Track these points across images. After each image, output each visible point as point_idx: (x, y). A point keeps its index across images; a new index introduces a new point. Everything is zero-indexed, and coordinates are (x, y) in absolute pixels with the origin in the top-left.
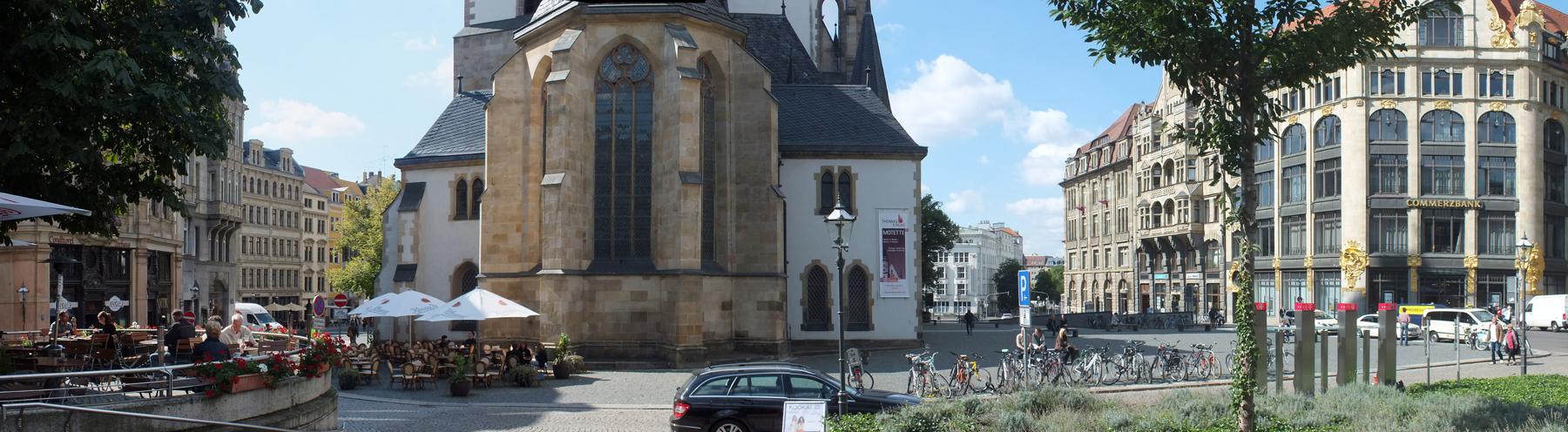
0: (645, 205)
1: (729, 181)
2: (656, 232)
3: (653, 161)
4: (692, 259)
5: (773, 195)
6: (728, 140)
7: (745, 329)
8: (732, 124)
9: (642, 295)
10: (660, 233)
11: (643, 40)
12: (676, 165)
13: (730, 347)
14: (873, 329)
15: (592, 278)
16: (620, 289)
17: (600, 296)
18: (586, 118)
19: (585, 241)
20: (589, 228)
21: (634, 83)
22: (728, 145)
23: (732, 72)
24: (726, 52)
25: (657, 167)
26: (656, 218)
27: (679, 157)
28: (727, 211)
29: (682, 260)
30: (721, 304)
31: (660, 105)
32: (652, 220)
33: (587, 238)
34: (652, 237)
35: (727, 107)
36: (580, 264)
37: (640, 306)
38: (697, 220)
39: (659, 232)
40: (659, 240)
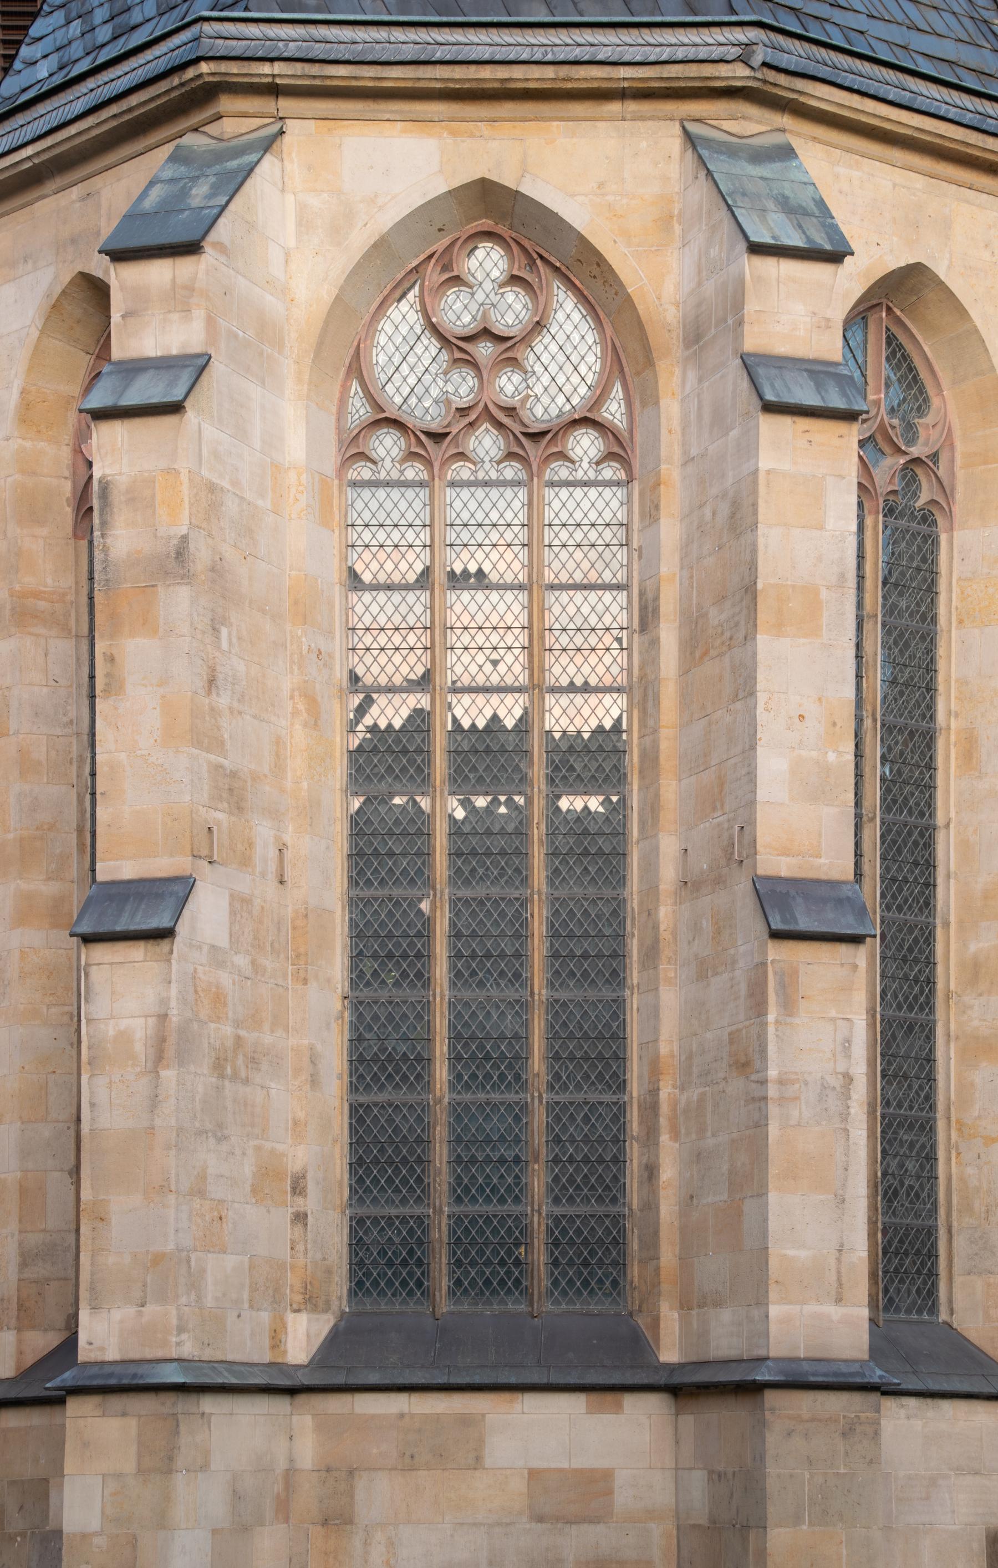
2: (651, 1171)
4: (834, 1312)
16: (478, 1463)
19: (300, 1218)
21: (536, 437)
26: (651, 1107)
27: (752, 803)
29: (775, 1311)
33: (311, 1203)
34: (634, 1196)
36: (277, 1337)
38: (845, 1116)
39: (668, 1173)
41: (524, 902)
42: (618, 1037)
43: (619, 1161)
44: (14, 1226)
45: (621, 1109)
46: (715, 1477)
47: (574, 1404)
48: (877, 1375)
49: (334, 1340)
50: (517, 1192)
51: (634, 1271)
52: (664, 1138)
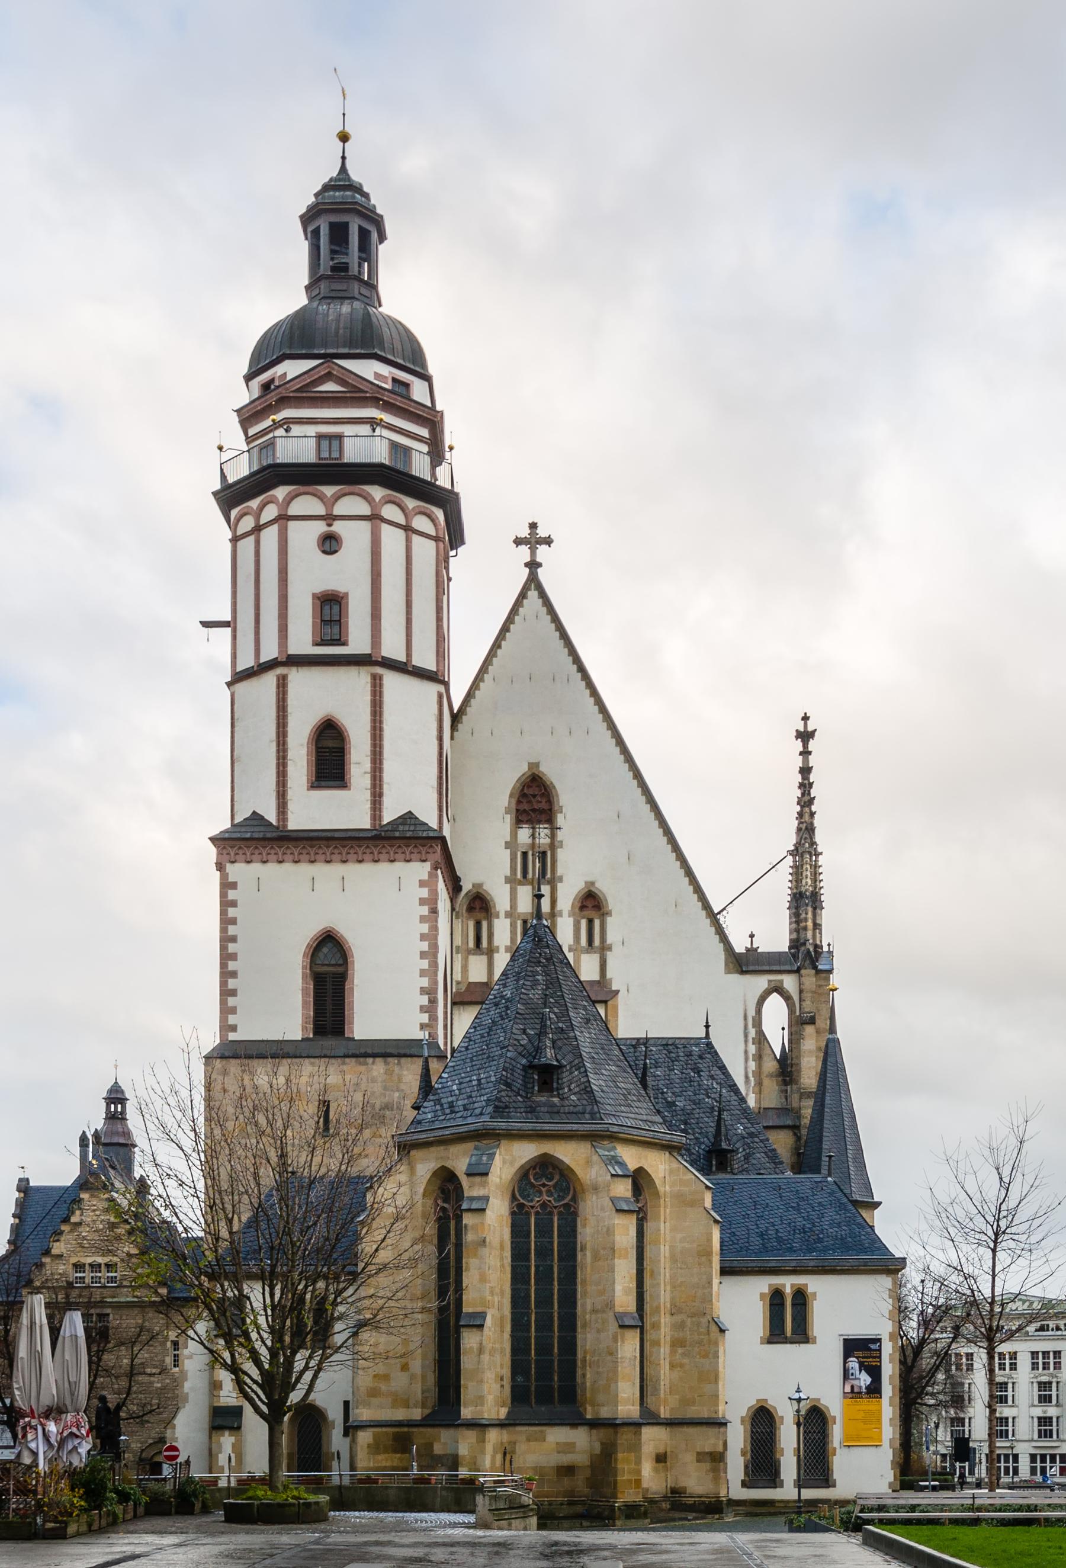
0: (569, 1346)
1: (662, 1313)
2: (584, 1376)
3: (579, 1296)
5: (714, 1328)
6: (662, 1265)
7: (683, 1485)
8: (667, 1247)
9: (567, 1448)
10: (588, 1377)
11: (567, 1160)
12: (610, 1305)
13: (665, 1505)
14: (834, 1486)
15: (511, 1429)
17: (521, 1447)
18: (502, 1248)
19: (502, 1386)
20: (507, 1372)
22: (662, 1270)
23: (668, 1188)
24: (662, 1167)
25: (586, 1303)
26: (584, 1360)
28: (659, 1345)
30: (654, 1457)
31: (586, 1233)
32: (579, 1363)
34: (579, 1380)
35: (662, 1228)
36: (498, 1412)
37: (566, 1459)
38: (635, 1365)
39: (588, 1376)
40: (588, 1384)
41: (552, 1313)
42: (575, 1345)
43: (575, 1372)
44: (420, 1384)
45: (575, 1362)
46: (602, 1444)
47: (568, 1428)
48: (641, 1421)
49: (509, 1413)
50: (552, 1379)
51: (579, 1397)
52: (588, 1368)
